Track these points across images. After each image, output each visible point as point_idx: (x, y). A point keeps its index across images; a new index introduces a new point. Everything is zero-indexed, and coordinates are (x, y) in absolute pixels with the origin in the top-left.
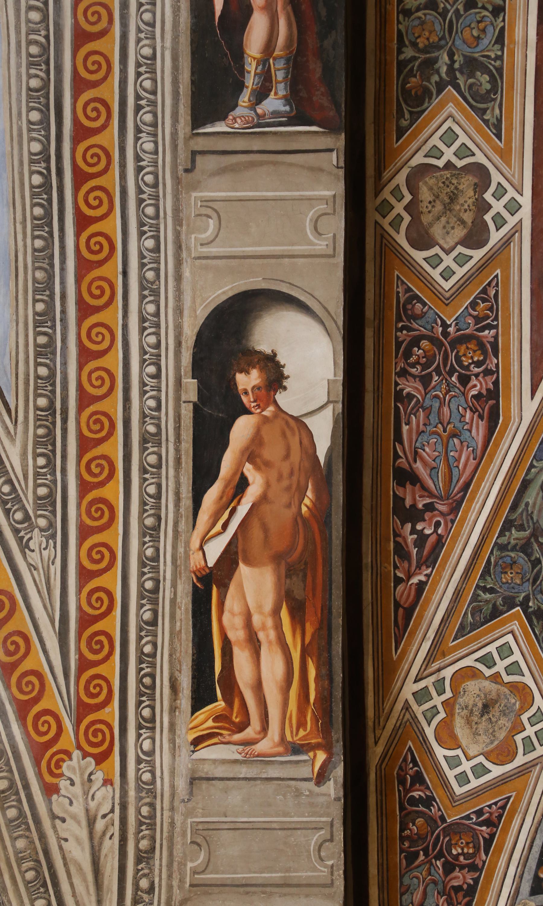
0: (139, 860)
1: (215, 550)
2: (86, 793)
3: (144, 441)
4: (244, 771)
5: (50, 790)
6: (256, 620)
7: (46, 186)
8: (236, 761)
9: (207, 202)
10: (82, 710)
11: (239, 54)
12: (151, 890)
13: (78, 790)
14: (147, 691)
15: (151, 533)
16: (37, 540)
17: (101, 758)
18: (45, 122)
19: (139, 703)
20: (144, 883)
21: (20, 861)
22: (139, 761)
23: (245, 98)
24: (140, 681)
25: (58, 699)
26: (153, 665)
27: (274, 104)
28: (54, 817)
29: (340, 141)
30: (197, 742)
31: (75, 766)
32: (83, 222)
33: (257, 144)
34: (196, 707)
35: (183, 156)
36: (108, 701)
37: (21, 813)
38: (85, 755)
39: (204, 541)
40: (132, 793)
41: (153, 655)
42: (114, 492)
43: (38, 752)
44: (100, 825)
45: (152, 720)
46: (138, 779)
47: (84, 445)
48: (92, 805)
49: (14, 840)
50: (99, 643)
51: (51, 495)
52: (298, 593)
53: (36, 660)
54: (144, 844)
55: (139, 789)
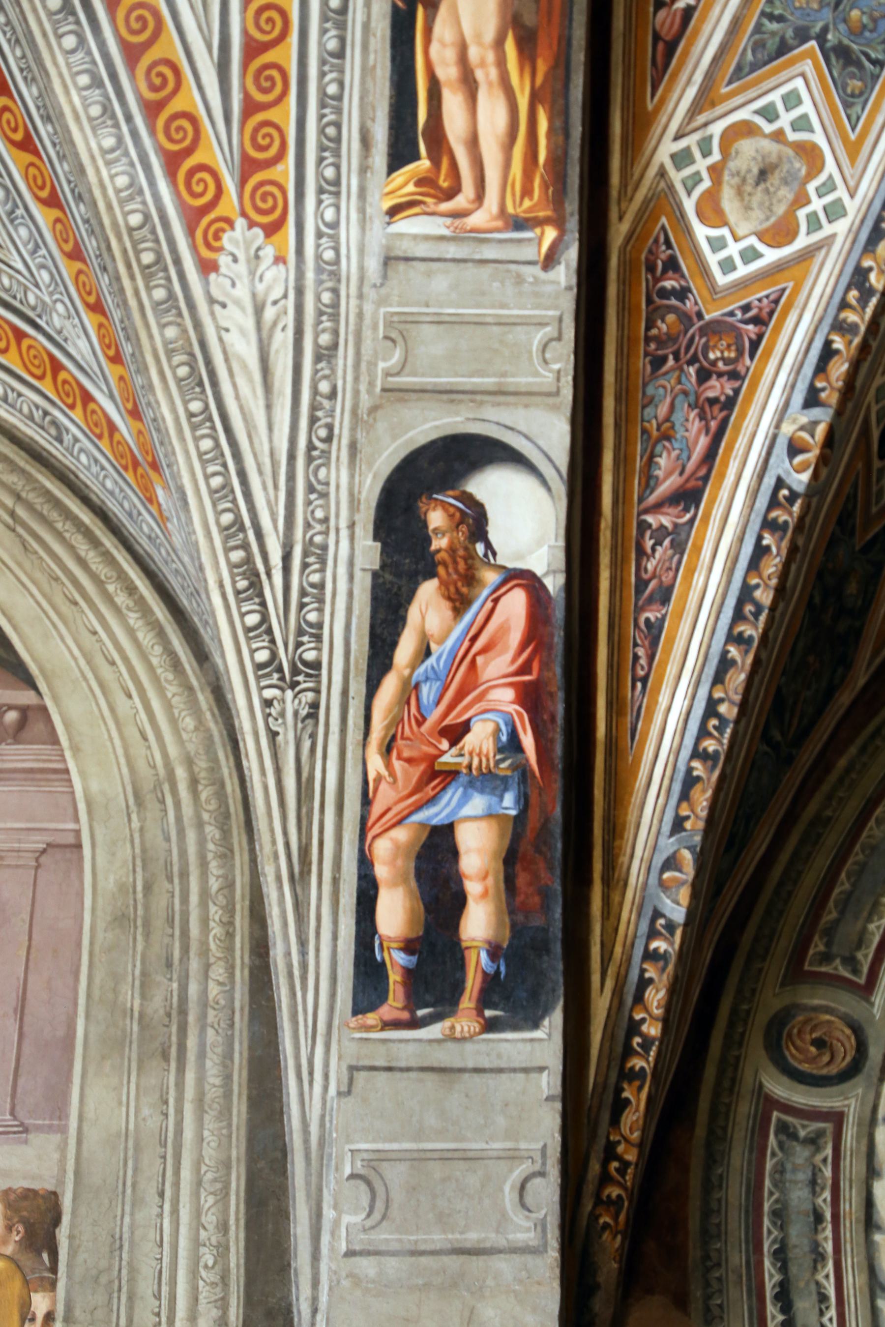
0: (318, 358)
2: (252, 273)
4: (452, 251)
5: (207, 267)
6: (474, 53)
8: (442, 238)
10: (248, 167)
12: (333, 395)
13: (242, 268)
14: (331, 145)
17: (272, 229)
19: (320, 160)
20: (324, 387)
21: (170, 353)
22: (319, 235)
24: (322, 131)
26: (339, 111)
28: (212, 301)
30: (394, 211)
31: (239, 238)
34: (392, 168)
36: (280, 156)
37: (171, 296)
38: (252, 224)
40: (310, 275)
41: (339, 98)
43: (193, 218)
44: (270, 313)
45: (337, 182)
46: (318, 257)
48: (260, 288)
49: (162, 326)
52: (529, 19)
53: (189, 99)
54: (325, 339)
55: (319, 270)
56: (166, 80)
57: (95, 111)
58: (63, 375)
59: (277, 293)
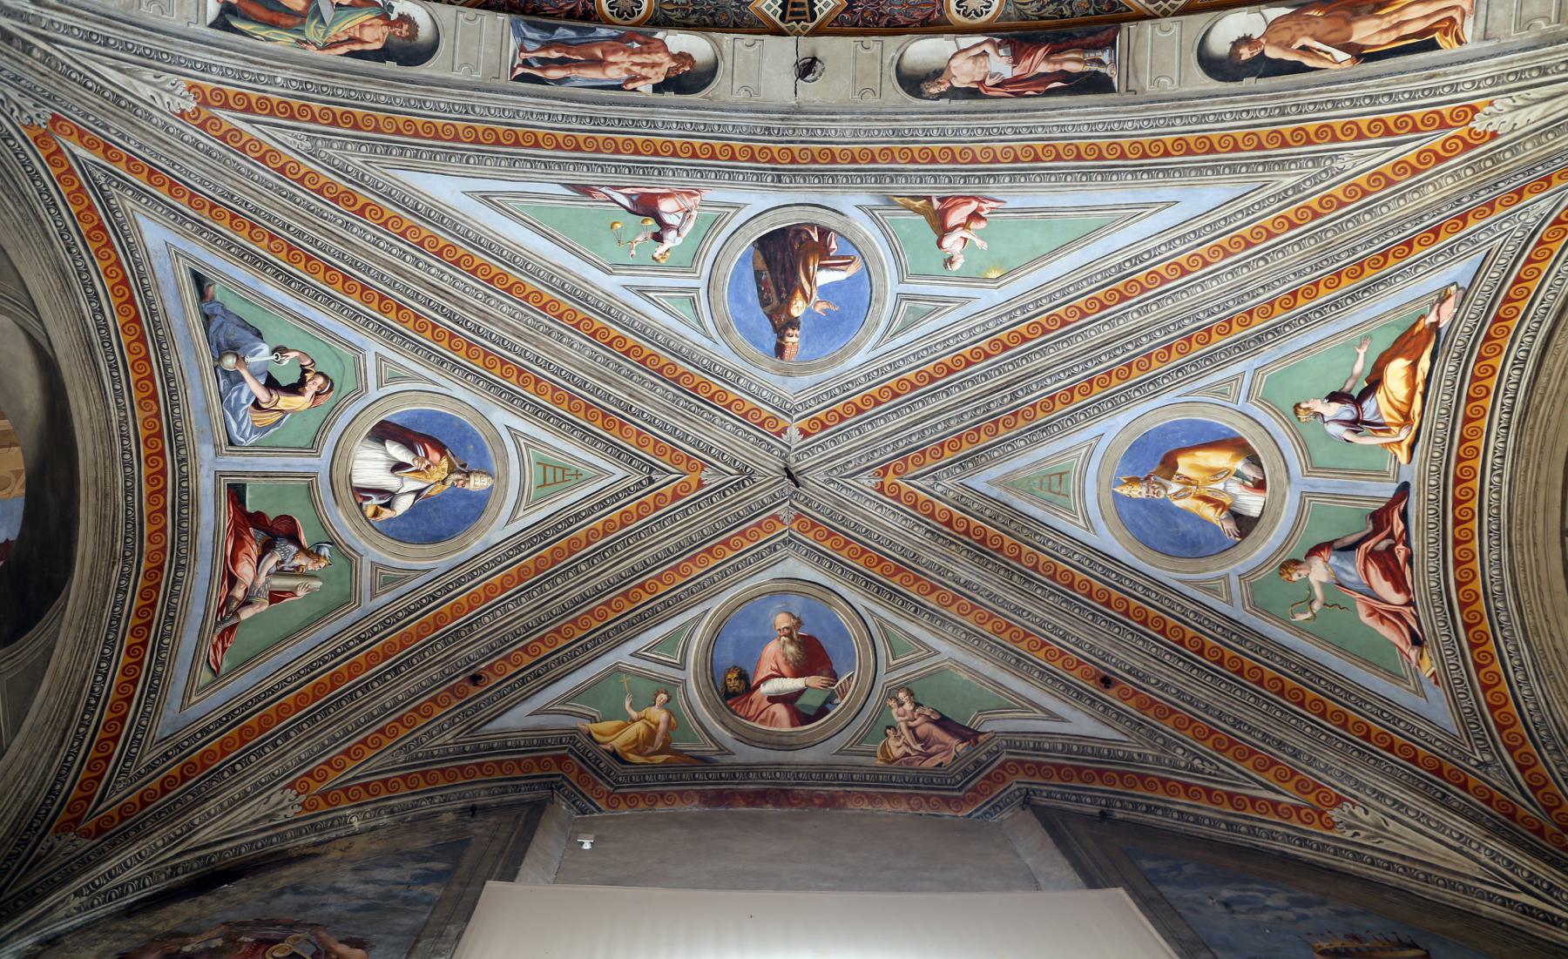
0: (1546, 74)
1: (1341, 56)
3: (1283, 115)
4: (1482, 12)
6: (1384, 26)
7: (1148, 172)
9: (1151, 83)
10: (1444, 125)
11: (1082, 74)
13: (1495, 120)
14: (1433, 91)
15: (1336, 104)
16: (1338, 165)
17: (1475, 110)
18: (1117, 173)
23: (1102, 70)
25: (1435, 140)
27: (1105, 56)
28: (1513, 130)
29: (1125, 25)
30: (1460, 42)
31: (1479, 124)
32: (1167, 154)
33: (1124, 63)
35: (1129, 95)
36: (1438, 112)
39: (1336, 62)
42: (1311, 127)
43: (1468, 147)
44: (1520, 103)
47: (1285, 144)
50: (1400, 124)
51: (1312, 159)
52: (1371, 7)
53: (1411, 157)
56: (1402, 167)
57: (1416, 196)
58: (1563, 217)
59: (1509, 101)
